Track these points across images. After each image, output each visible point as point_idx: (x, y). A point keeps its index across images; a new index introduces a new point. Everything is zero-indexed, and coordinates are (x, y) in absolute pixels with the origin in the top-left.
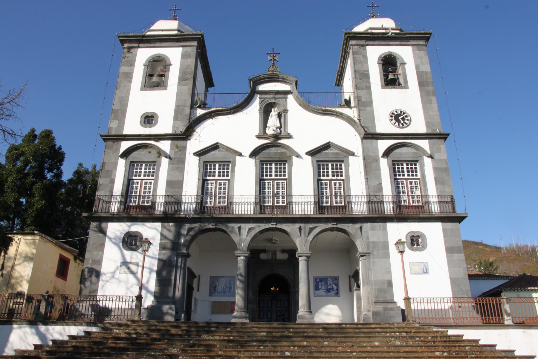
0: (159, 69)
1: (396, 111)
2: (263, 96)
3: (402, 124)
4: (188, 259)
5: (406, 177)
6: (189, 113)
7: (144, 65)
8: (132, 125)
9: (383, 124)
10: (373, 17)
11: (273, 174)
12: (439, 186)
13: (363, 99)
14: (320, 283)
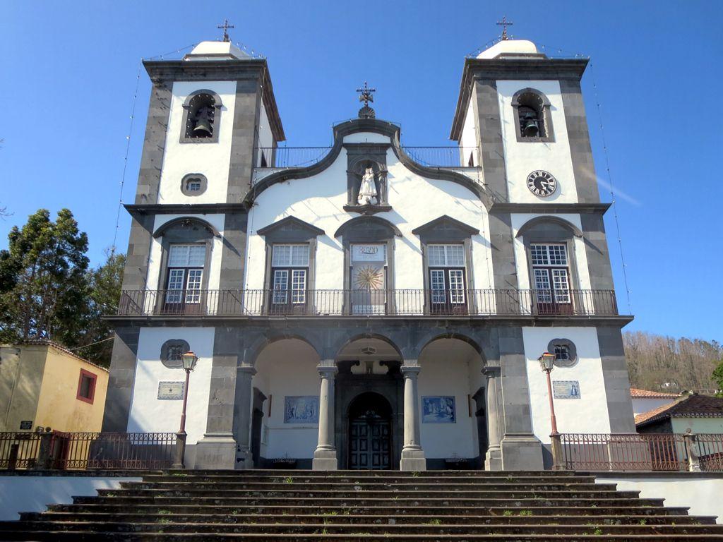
0: (205, 111)
1: (537, 174)
2: (354, 152)
3: (546, 192)
4: (253, 377)
5: (549, 265)
6: (250, 176)
7: (184, 107)
9: (520, 193)
10: (504, 39)
12: (594, 277)
14: (430, 405)
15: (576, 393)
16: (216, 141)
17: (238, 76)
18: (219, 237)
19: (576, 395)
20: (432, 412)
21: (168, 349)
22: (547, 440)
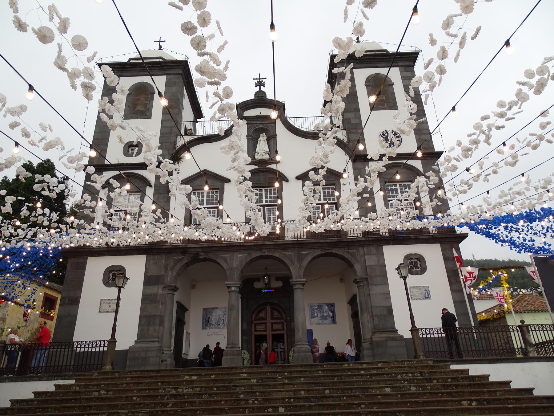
4: (175, 293)
8: (115, 154)
11: (264, 200)
13: (353, 121)
15: (428, 295)
16: (150, 117)
17: (167, 72)
18: (151, 186)
19: (429, 297)
20: (317, 316)
21: (109, 274)
22: (408, 335)
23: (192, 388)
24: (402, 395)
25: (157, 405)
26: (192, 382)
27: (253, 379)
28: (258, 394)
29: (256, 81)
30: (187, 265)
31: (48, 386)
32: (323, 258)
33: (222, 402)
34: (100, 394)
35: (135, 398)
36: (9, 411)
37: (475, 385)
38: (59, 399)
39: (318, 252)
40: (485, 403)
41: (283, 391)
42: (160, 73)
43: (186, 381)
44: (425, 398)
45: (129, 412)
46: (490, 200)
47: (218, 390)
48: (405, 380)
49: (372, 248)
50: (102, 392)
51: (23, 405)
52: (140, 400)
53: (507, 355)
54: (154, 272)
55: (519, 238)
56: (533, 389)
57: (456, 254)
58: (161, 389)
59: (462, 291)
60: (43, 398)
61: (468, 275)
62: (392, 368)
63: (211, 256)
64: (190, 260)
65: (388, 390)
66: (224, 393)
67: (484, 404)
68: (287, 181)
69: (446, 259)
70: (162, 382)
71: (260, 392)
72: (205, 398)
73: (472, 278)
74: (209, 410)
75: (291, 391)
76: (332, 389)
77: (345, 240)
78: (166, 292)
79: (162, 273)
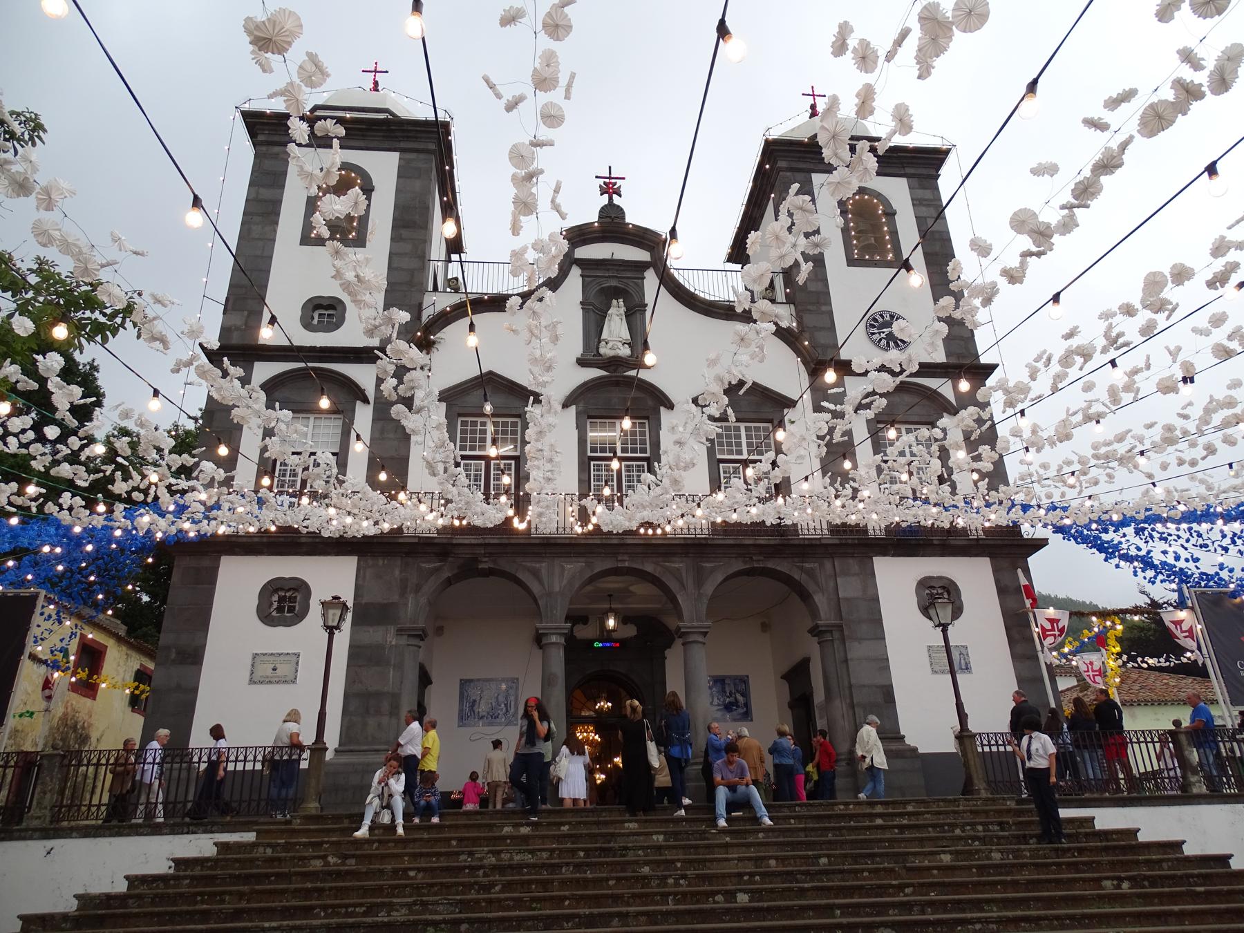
4: (421, 643)
17: (402, 145)
23: (532, 852)
24: (979, 867)
25: (468, 887)
26: (525, 839)
27: (657, 833)
28: (679, 865)
29: (601, 181)
30: (449, 582)
31: (201, 845)
32: (745, 577)
33: (611, 883)
34: (327, 864)
35: (412, 874)
36: (131, 901)
37: (1115, 847)
38: (240, 875)
39: (738, 566)
40: (1146, 883)
41: (733, 859)
42: (386, 146)
43: (512, 837)
44: (1025, 876)
45: (415, 903)
46: (1210, 480)
47: (587, 856)
48: (974, 838)
49: (851, 561)
50: (331, 860)
51: (157, 887)
52: (423, 878)
53: (1142, 792)
54: (376, 595)
55: (1165, 552)
56: (1230, 856)
57: (1023, 581)
58: (463, 853)
59: (1035, 658)
60: (197, 871)
61: (1048, 626)
62: (939, 813)
63: (504, 564)
64: (456, 571)
65: (946, 858)
66: (607, 863)
67: (1144, 887)
68: (670, 406)
69: (1002, 591)
70: (460, 840)
71: (684, 861)
72: (566, 873)
73: (1057, 633)
74: (589, 897)
75: (749, 859)
76: (833, 855)
77: (797, 542)
78: (403, 641)
79: (395, 598)
